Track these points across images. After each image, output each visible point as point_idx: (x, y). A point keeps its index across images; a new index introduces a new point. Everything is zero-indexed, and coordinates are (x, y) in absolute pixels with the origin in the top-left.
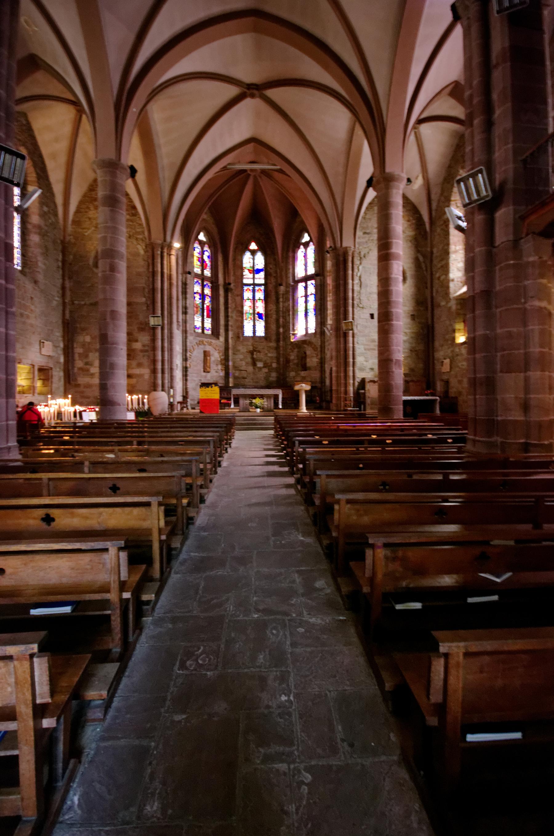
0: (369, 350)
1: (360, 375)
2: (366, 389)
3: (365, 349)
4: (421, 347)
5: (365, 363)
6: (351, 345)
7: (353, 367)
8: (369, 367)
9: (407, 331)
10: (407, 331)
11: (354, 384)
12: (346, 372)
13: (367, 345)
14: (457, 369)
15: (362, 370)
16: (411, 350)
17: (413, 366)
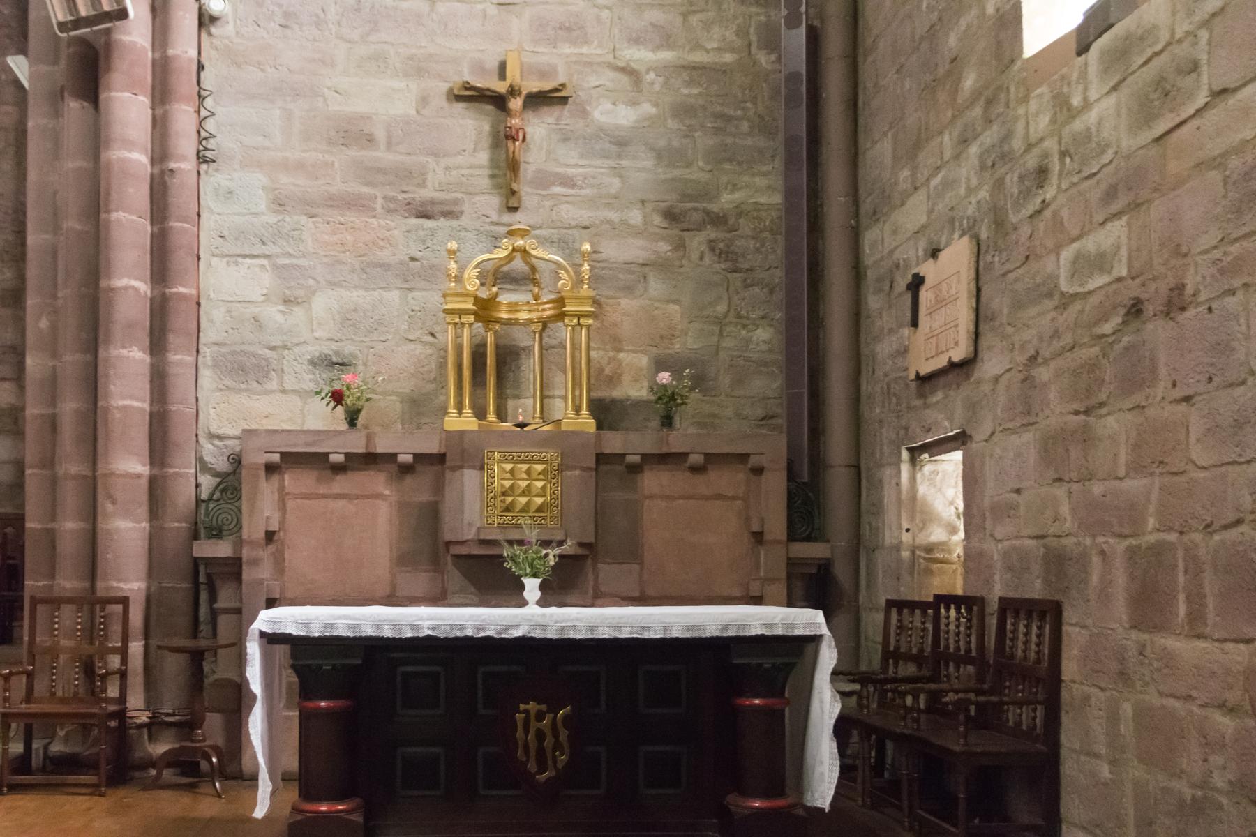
0: (309, 206)
1: (228, 414)
2: (253, 529)
3: (279, 204)
4: (760, 190)
5: (273, 314)
6: (139, 158)
7: (158, 343)
8: (315, 350)
9: (640, 56)
10: (640, 56)
11: (157, 491)
12: (93, 383)
13: (300, 166)
14: (1041, 318)
15: (246, 369)
16: (671, 216)
17: (688, 343)
